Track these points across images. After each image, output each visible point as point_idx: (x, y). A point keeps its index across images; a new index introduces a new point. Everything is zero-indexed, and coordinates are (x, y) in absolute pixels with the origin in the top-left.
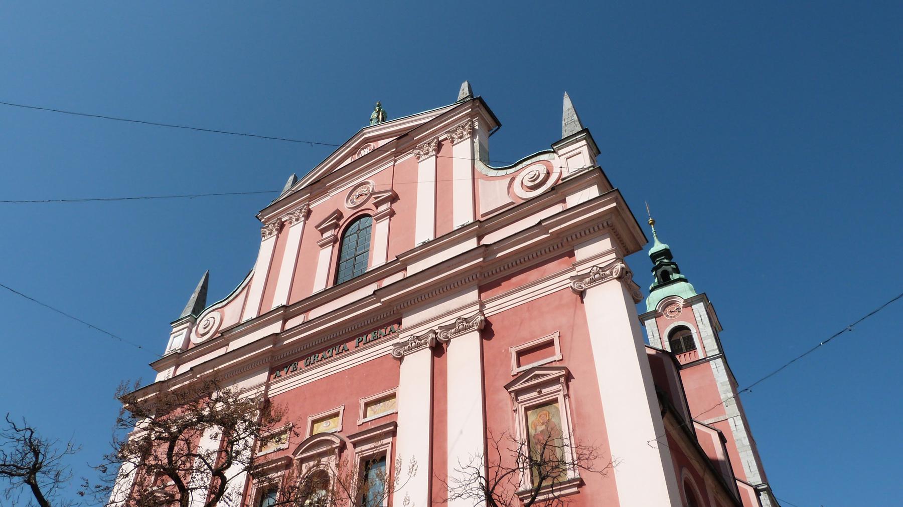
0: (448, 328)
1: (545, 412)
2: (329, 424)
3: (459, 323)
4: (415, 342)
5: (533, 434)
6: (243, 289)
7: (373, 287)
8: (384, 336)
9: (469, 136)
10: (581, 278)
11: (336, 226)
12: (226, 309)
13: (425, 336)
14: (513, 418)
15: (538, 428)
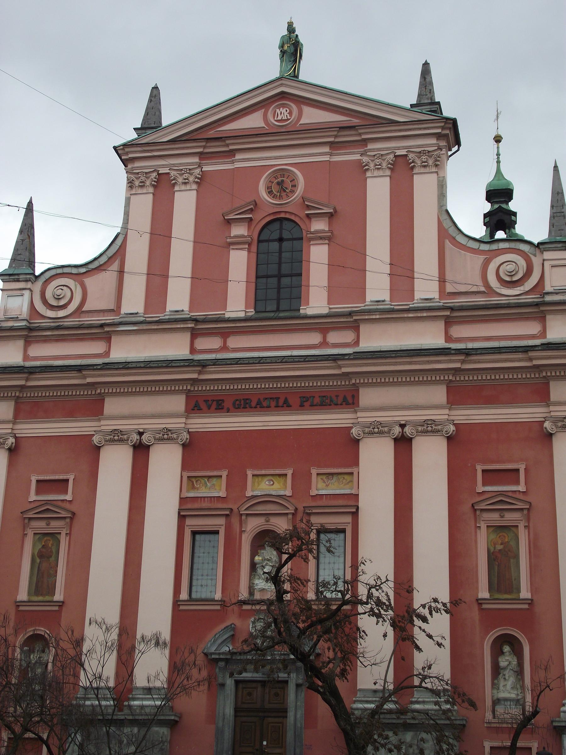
0: (416, 424)
1: (504, 534)
2: (272, 483)
3: (428, 424)
4: (378, 428)
5: (492, 551)
6: (111, 259)
7: (315, 338)
8: (337, 405)
9: (434, 169)
10: (555, 421)
12: (89, 281)
13: (390, 426)
14: (476, 532)
15: (497, 546)
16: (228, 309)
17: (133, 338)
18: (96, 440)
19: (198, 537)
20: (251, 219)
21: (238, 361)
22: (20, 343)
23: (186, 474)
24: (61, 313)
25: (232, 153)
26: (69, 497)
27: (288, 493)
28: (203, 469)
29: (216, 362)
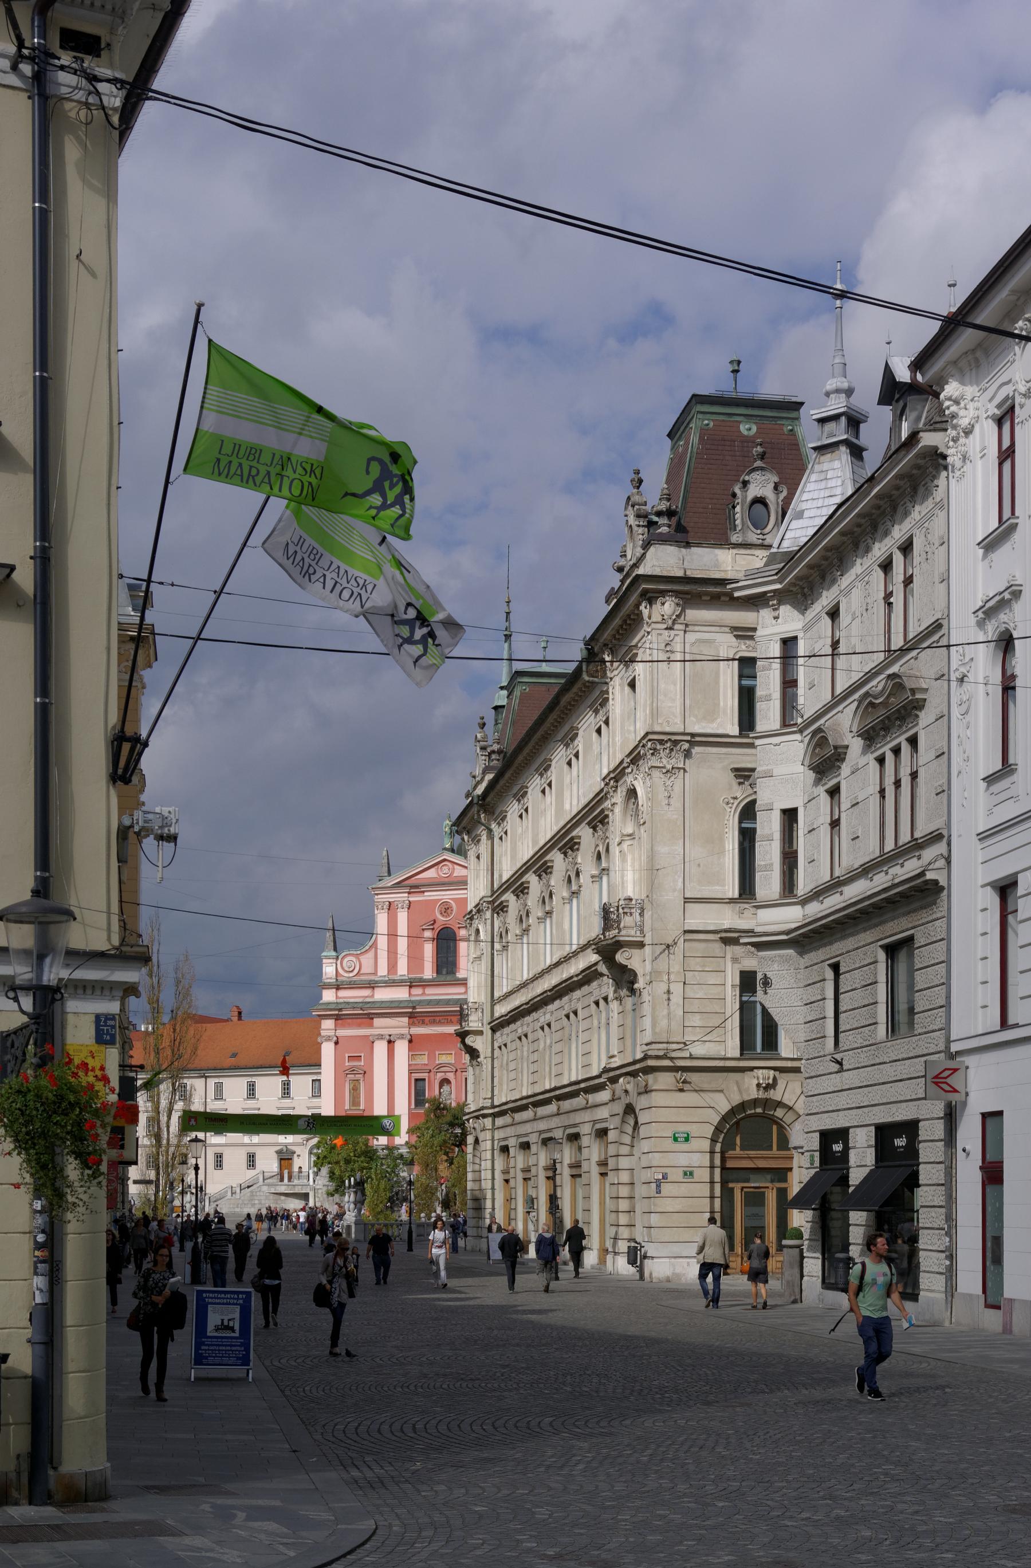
11: (433, 929)
12: (362, 958)
16: (425, 973)
17: (383, 989)
18: (371, 1038)
19: (419, 1082)
20: (433, 929)
21: (429, 1003)
22: (334, 990)
23: (411, 1053)
24: (351, 975)
25: (423, 892)
26: (362, 1064)
27: (453, 1062)
28: (418, 1051)
29: (420, 1002)
